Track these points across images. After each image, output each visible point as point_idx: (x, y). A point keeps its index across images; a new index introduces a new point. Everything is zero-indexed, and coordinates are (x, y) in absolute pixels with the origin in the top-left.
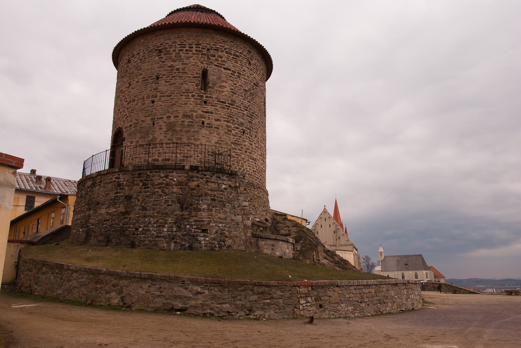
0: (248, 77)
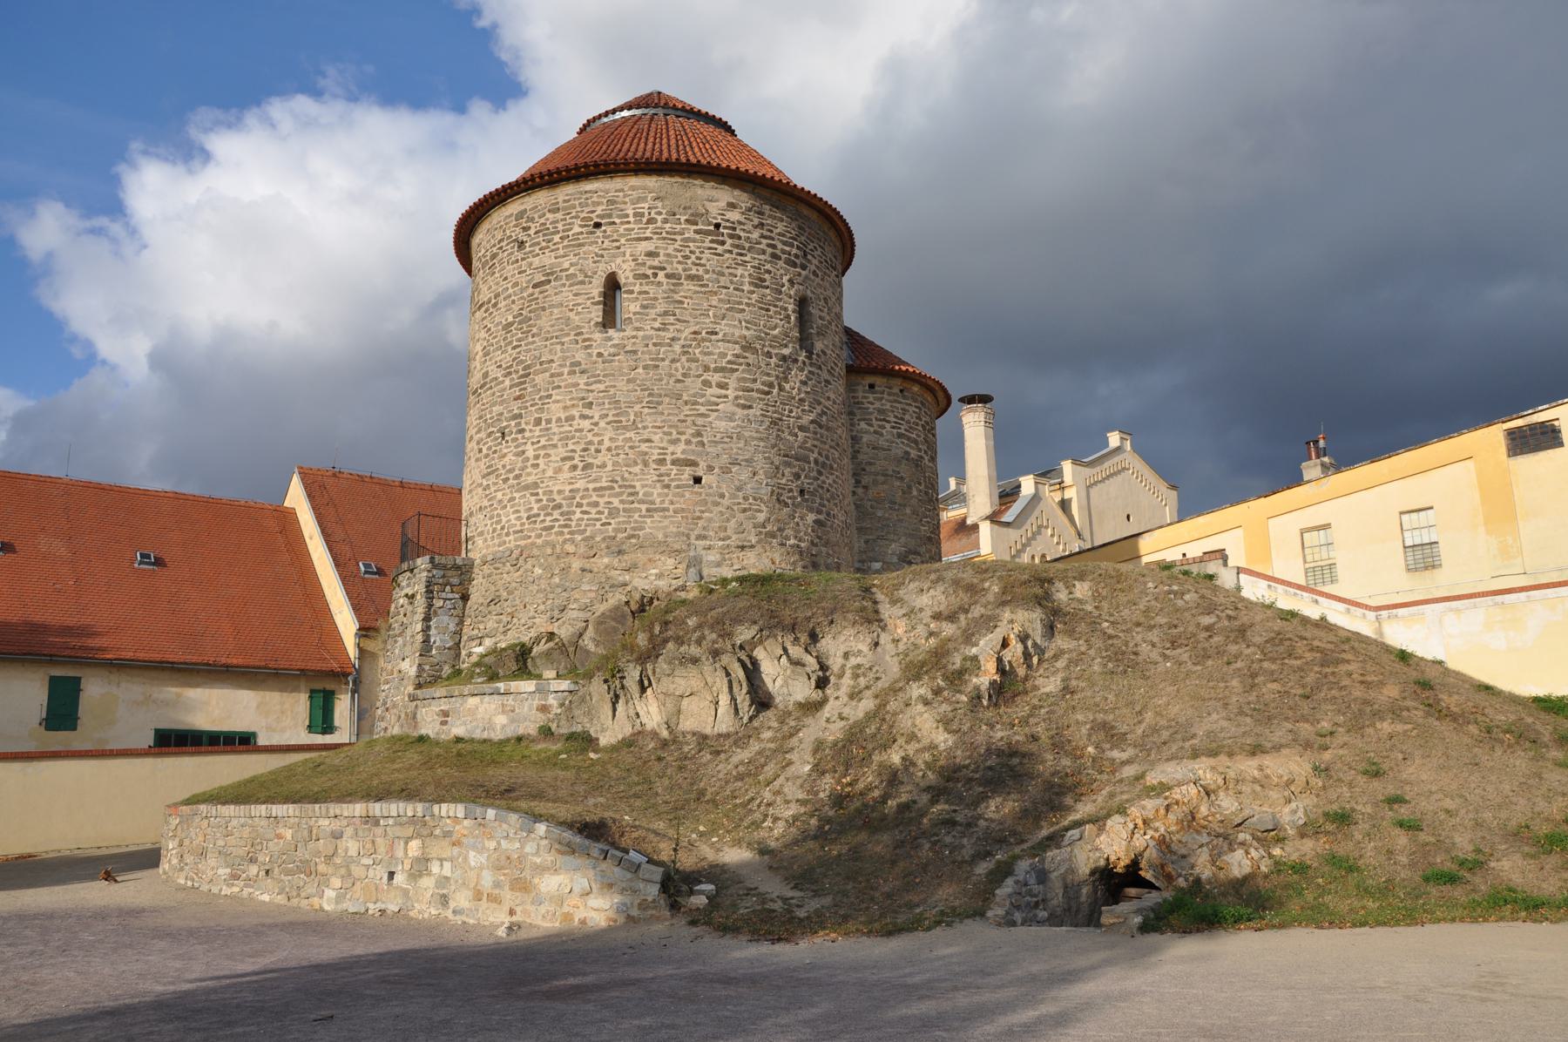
0: (516, 284)
